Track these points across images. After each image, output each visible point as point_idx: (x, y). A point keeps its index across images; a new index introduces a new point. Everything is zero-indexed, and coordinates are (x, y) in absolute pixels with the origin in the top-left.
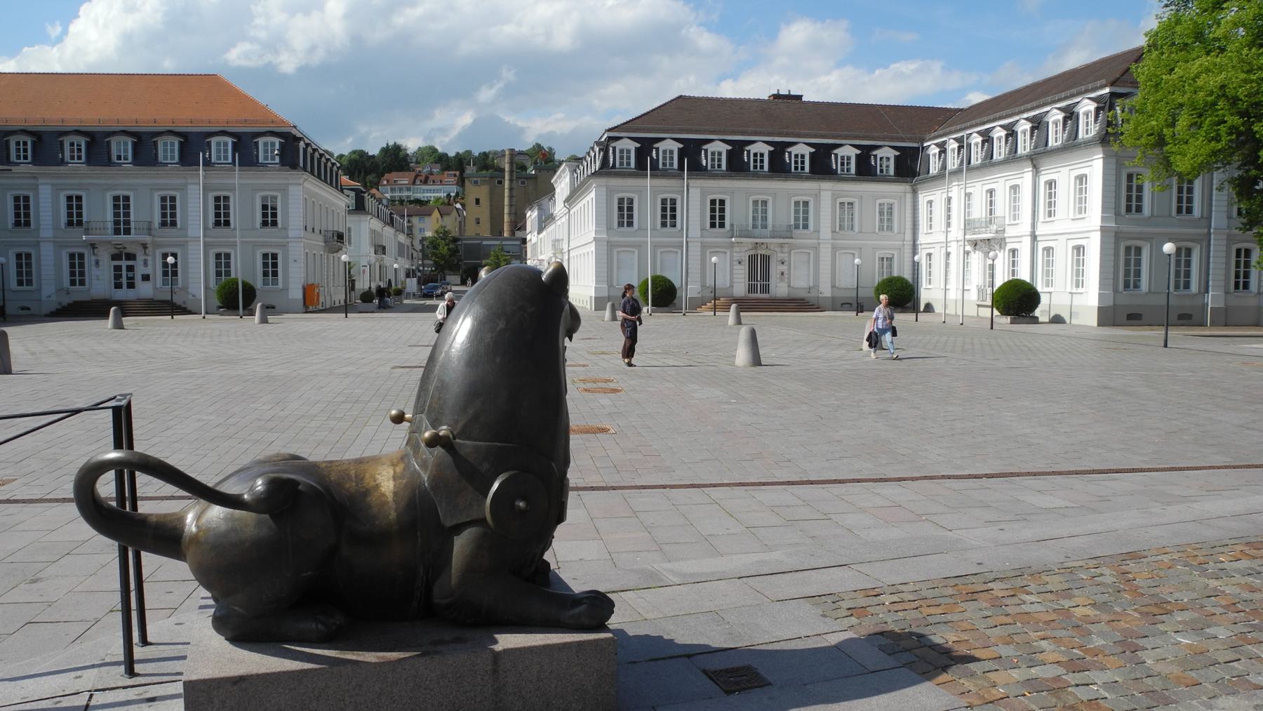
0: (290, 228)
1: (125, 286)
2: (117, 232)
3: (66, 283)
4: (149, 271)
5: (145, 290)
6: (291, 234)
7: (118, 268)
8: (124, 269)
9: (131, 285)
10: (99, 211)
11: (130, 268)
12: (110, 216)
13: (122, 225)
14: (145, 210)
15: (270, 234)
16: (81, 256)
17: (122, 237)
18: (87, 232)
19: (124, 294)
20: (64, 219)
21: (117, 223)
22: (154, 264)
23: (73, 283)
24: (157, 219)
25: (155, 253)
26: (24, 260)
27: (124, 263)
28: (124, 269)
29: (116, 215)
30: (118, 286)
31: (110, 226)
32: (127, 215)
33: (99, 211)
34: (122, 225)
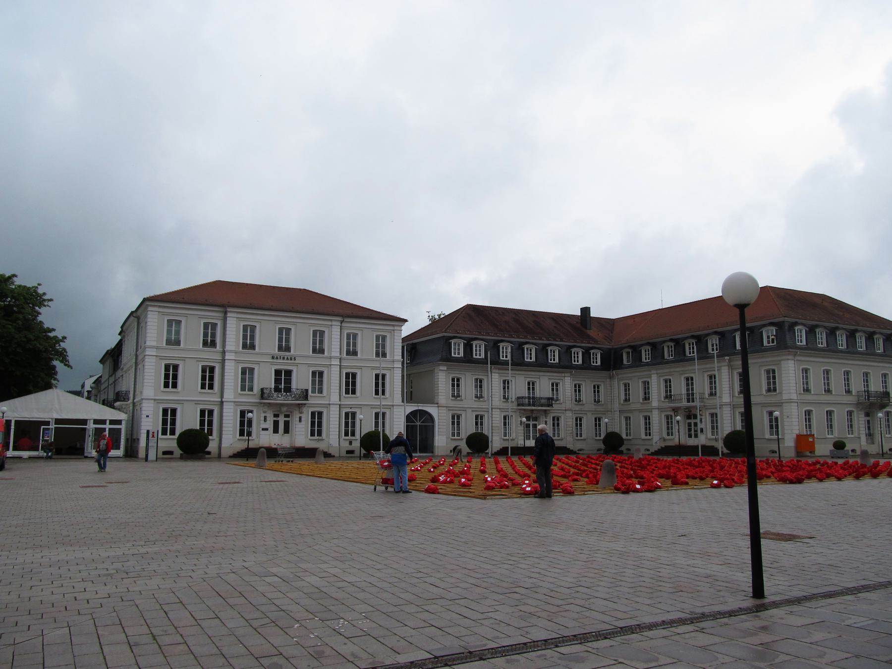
0: (784, 392)
1: (693, 436)
2: (688, 401)
3: (665, 435)
4: (703, 426)
5: (702, 440)
6: (785, 397)
7: (690, 425)
8: (692, 424)
9: (696, 436)
10: (679, 388)
11: (696, 424)
12: (684, 391)
13: (690, 397)
14: (701, 386)
15: (772, 398)
16: (671, 416)
17: (691, 404)
18: (672, 401)
19: (692, 442)
20: (663, 394)
21: (688, 395)
22: (706, 422)
23: (668, 435)
24: (707, 391)
25: (706, 414)
26: (647, 419)
27: (692, 421)
28: (692, 424)
29: (688, 390)
30: (690, 436)
31: (684, 397)
32: (692, 389)
33: (679, 388)
34: (690, 397)
